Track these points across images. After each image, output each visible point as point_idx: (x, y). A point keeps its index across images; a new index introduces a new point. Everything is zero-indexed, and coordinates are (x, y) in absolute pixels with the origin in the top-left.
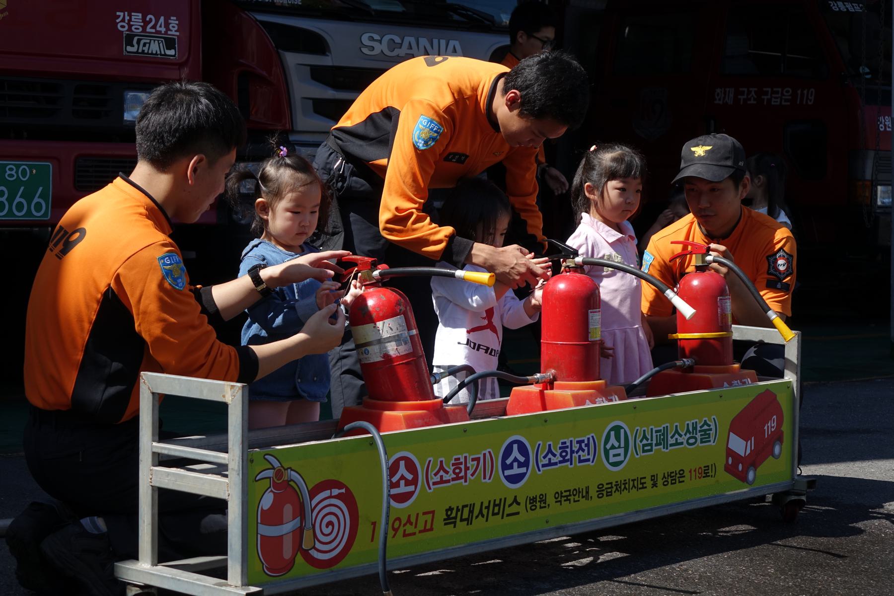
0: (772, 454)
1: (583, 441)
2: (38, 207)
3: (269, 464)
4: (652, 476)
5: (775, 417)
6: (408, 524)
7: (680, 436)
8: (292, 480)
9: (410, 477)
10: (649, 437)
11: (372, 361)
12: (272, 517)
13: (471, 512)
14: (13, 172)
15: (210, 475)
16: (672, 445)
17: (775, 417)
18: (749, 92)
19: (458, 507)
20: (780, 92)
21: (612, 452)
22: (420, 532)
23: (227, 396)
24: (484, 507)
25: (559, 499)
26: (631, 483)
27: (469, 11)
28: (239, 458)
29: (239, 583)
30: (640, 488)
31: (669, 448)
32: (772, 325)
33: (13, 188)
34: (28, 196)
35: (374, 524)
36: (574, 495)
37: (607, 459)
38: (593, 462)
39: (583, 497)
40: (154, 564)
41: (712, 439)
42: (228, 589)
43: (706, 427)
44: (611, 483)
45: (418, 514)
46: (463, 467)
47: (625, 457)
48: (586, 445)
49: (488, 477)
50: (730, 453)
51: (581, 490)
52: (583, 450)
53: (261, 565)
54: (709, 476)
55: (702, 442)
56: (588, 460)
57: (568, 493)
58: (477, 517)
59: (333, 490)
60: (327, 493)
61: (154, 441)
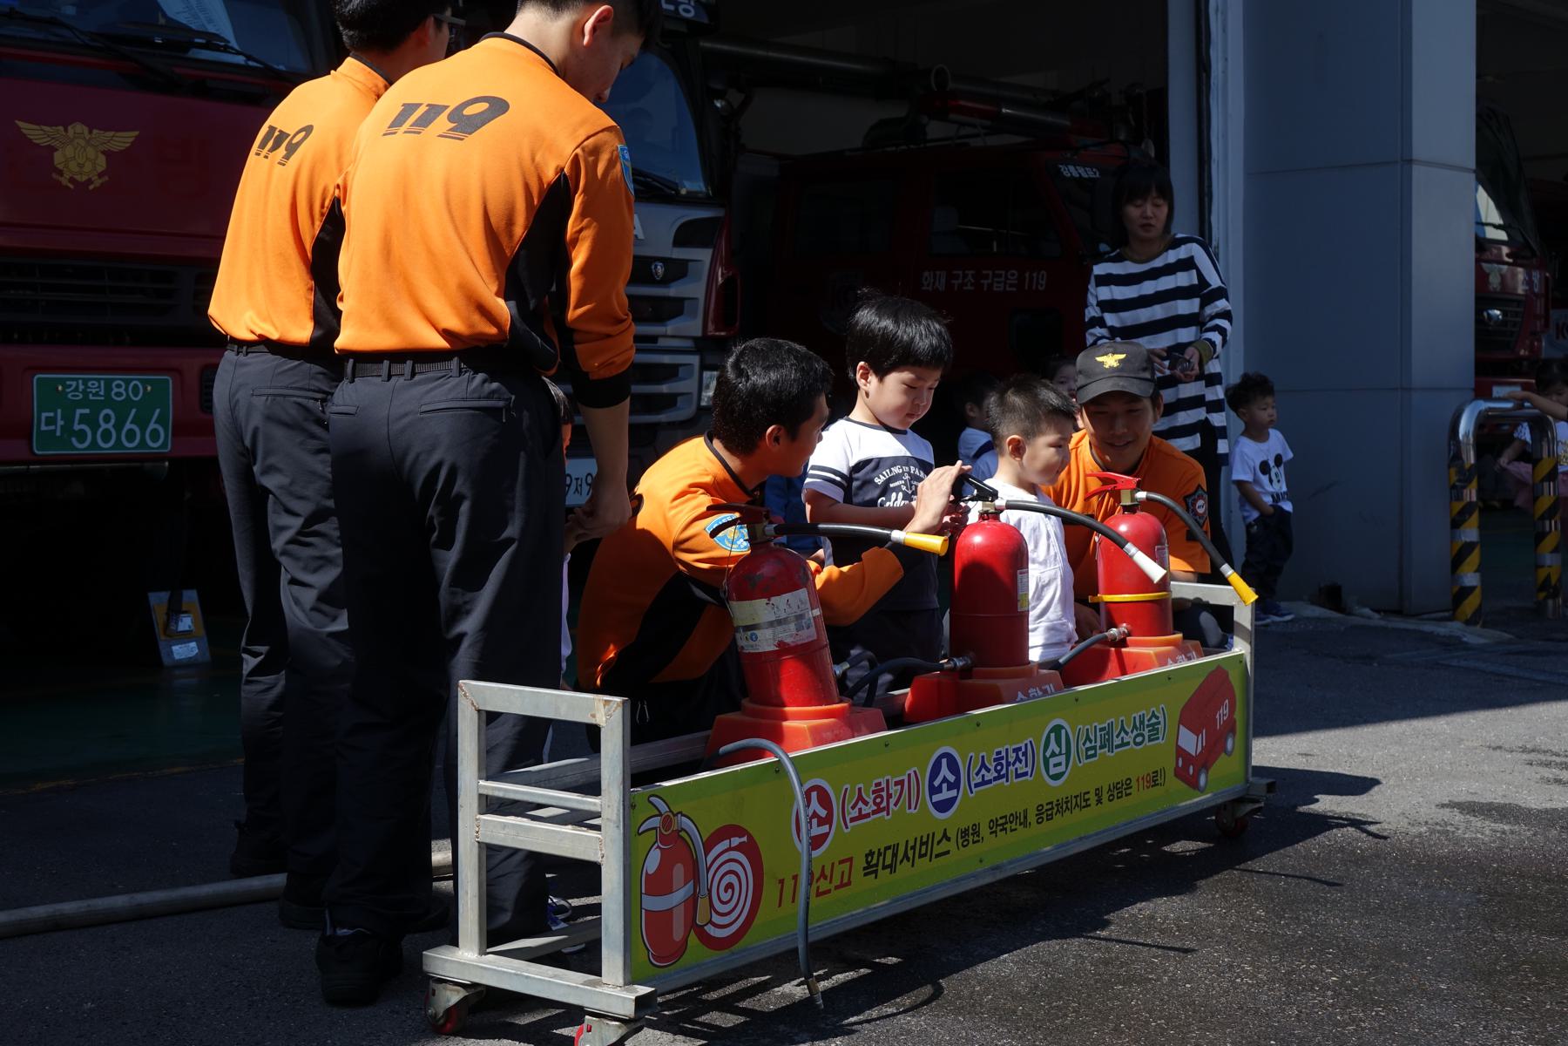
0: (1225, 750)
1: (1020, 749)
2: (155, 435)
3: (654, 808)
5: (1227, 701)
6: (822, 879)
7: (1127, 733)
8: (683, 830)
9: (823, 813)
10: (1093, 738)
11: (760, 651)
12: (659, 884)
13: (895, 855)
14: (122, 390)
15: (570, 827)
16: (1118, 747)
17: (1227, 701)
18: (965, 276)
19: (879, 850)
20: (1003, 276)
21: (1053, 761)
22: (837, 887)
23: (598, 716)
24: (909, 848)
25: (994, 829)
27: (649, 178)
28: (619, 803)
29: (621, 982)
30: (1084, 807)
31: (1115, 750)
32: (1225, 581)
33: (121, 410)
34: (142, 422)
35: (782, 882)
36: (1011, 822)
37: (1047, 771)
39: (1021, 824)
40: (483, 953)
41: (1160, 736)
42: (606, 990)
43: (1154, 720)
44: (1052, 803)
45: (833, 864)
46: (884, 794)
47: (1067, 768)
49: (913, 806)
50: (1180, 752)
52: (1020, 761)
53: (646, 952)
55: (1149, 741)
56: (1025, 774)
57: (1004, 820)
58: (902, 861)
59: (732, 839)
60: (724, 845)
61: (480, 778)
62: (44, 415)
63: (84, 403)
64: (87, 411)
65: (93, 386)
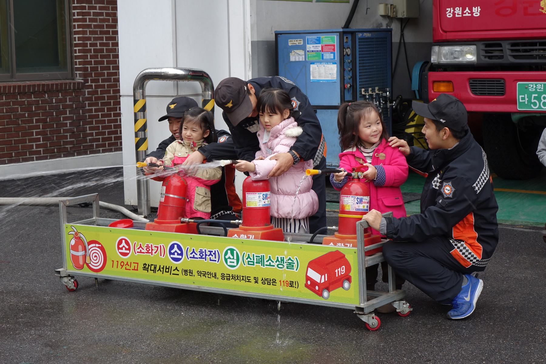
1: (212, 252)
4: (254, 277)
7: (273, 262)
22: (132, 270)
25: (200, 274)
26: (242, 278)
38: (218, 262)
39: (213, 277)
41: (295, 268)
43: (290, 261)
45: (131, 263)
48: (214, 254)
49: (162, 255)
50: (308, 278)
51: (211, 273)
52: (212, 256)
54: (294, 287)
56: (215, 261)
57: (204, 273)
58: (158, 271)
62: (520, 96)
63: (536, 92)
64: (536, 95)
65: (539, 86)
